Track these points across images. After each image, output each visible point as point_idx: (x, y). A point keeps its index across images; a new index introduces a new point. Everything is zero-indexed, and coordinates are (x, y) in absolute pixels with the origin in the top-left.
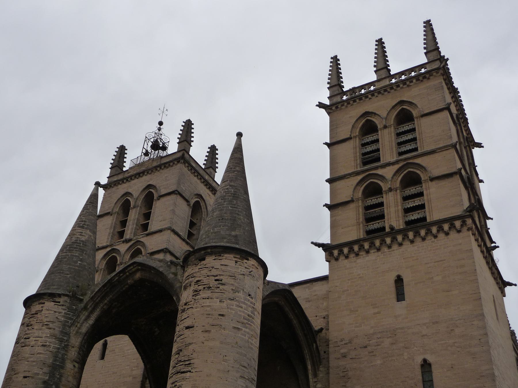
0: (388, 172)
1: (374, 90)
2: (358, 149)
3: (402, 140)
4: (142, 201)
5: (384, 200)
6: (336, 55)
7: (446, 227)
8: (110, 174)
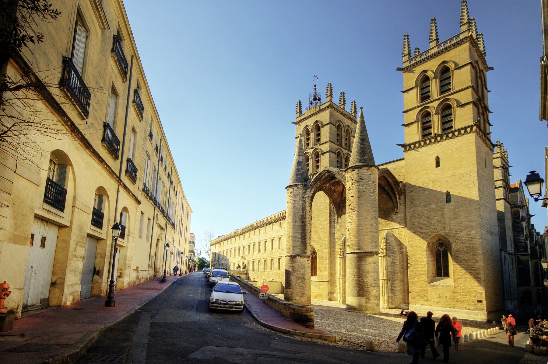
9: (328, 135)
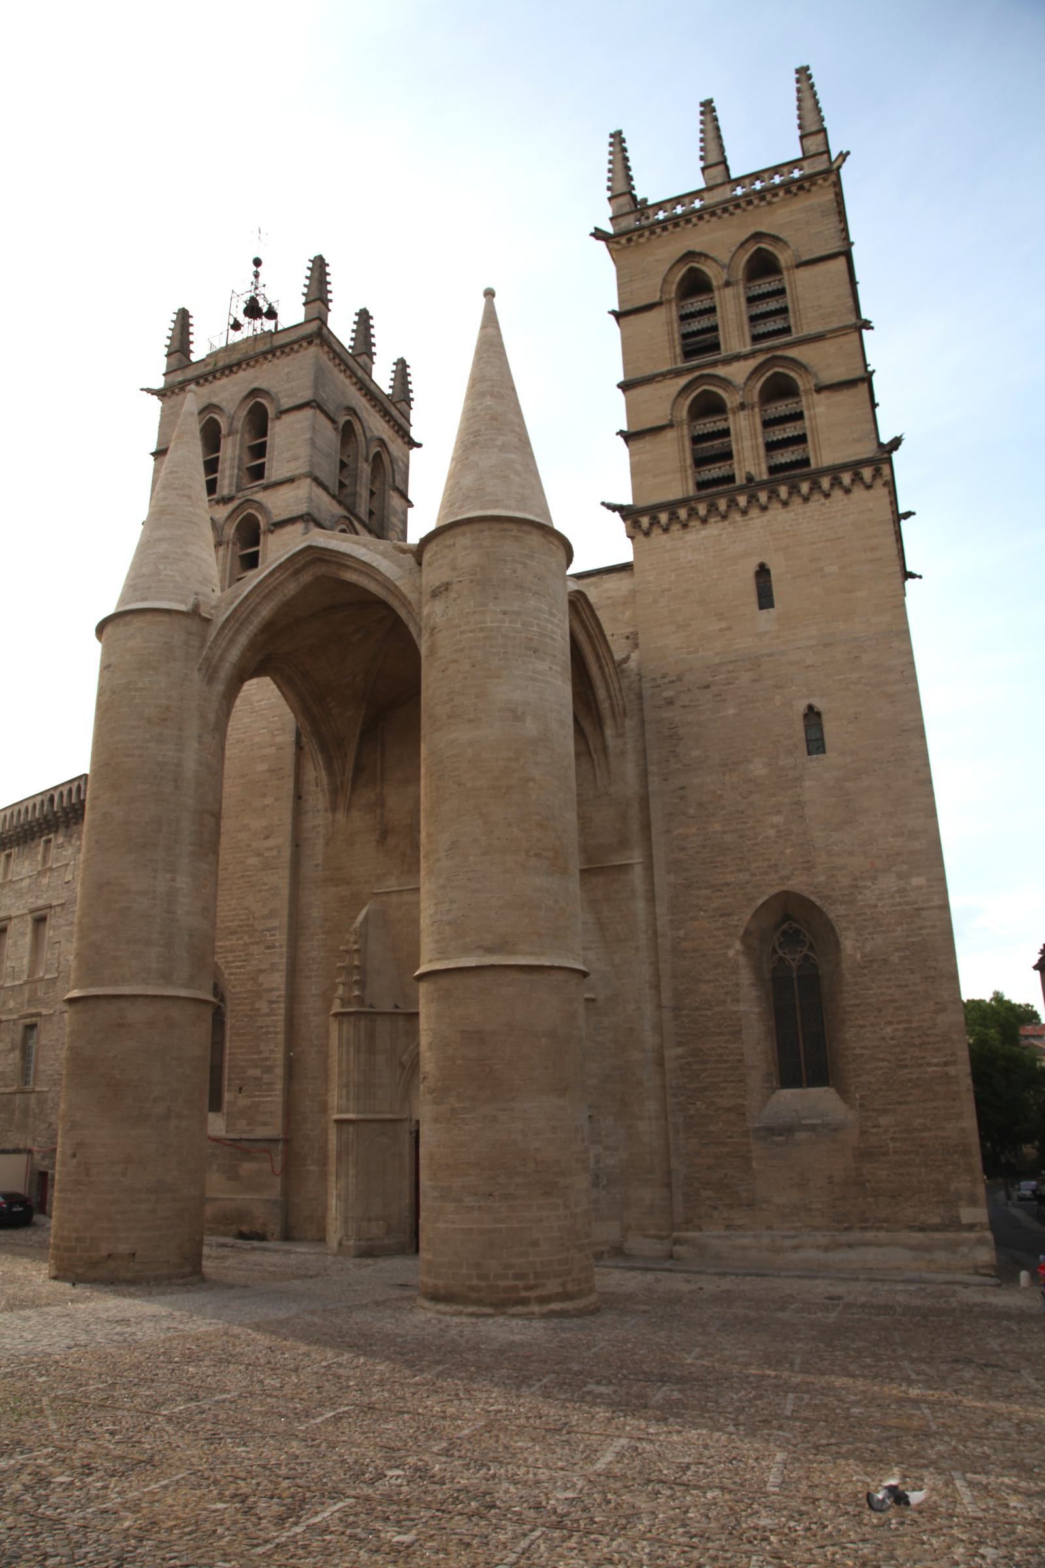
0: (738, 372)
1: (703, 209)
2: (675, 326)
3: (758, 311)
4: (244, 422)
5: (731, 423)
6: (619, 129)
7: (846, 478)
8: (167, 368)
9: (304, 451)
